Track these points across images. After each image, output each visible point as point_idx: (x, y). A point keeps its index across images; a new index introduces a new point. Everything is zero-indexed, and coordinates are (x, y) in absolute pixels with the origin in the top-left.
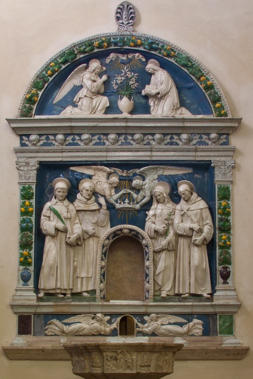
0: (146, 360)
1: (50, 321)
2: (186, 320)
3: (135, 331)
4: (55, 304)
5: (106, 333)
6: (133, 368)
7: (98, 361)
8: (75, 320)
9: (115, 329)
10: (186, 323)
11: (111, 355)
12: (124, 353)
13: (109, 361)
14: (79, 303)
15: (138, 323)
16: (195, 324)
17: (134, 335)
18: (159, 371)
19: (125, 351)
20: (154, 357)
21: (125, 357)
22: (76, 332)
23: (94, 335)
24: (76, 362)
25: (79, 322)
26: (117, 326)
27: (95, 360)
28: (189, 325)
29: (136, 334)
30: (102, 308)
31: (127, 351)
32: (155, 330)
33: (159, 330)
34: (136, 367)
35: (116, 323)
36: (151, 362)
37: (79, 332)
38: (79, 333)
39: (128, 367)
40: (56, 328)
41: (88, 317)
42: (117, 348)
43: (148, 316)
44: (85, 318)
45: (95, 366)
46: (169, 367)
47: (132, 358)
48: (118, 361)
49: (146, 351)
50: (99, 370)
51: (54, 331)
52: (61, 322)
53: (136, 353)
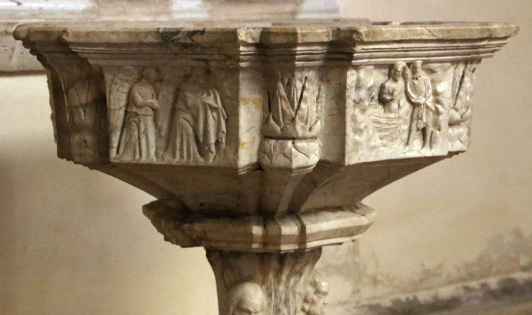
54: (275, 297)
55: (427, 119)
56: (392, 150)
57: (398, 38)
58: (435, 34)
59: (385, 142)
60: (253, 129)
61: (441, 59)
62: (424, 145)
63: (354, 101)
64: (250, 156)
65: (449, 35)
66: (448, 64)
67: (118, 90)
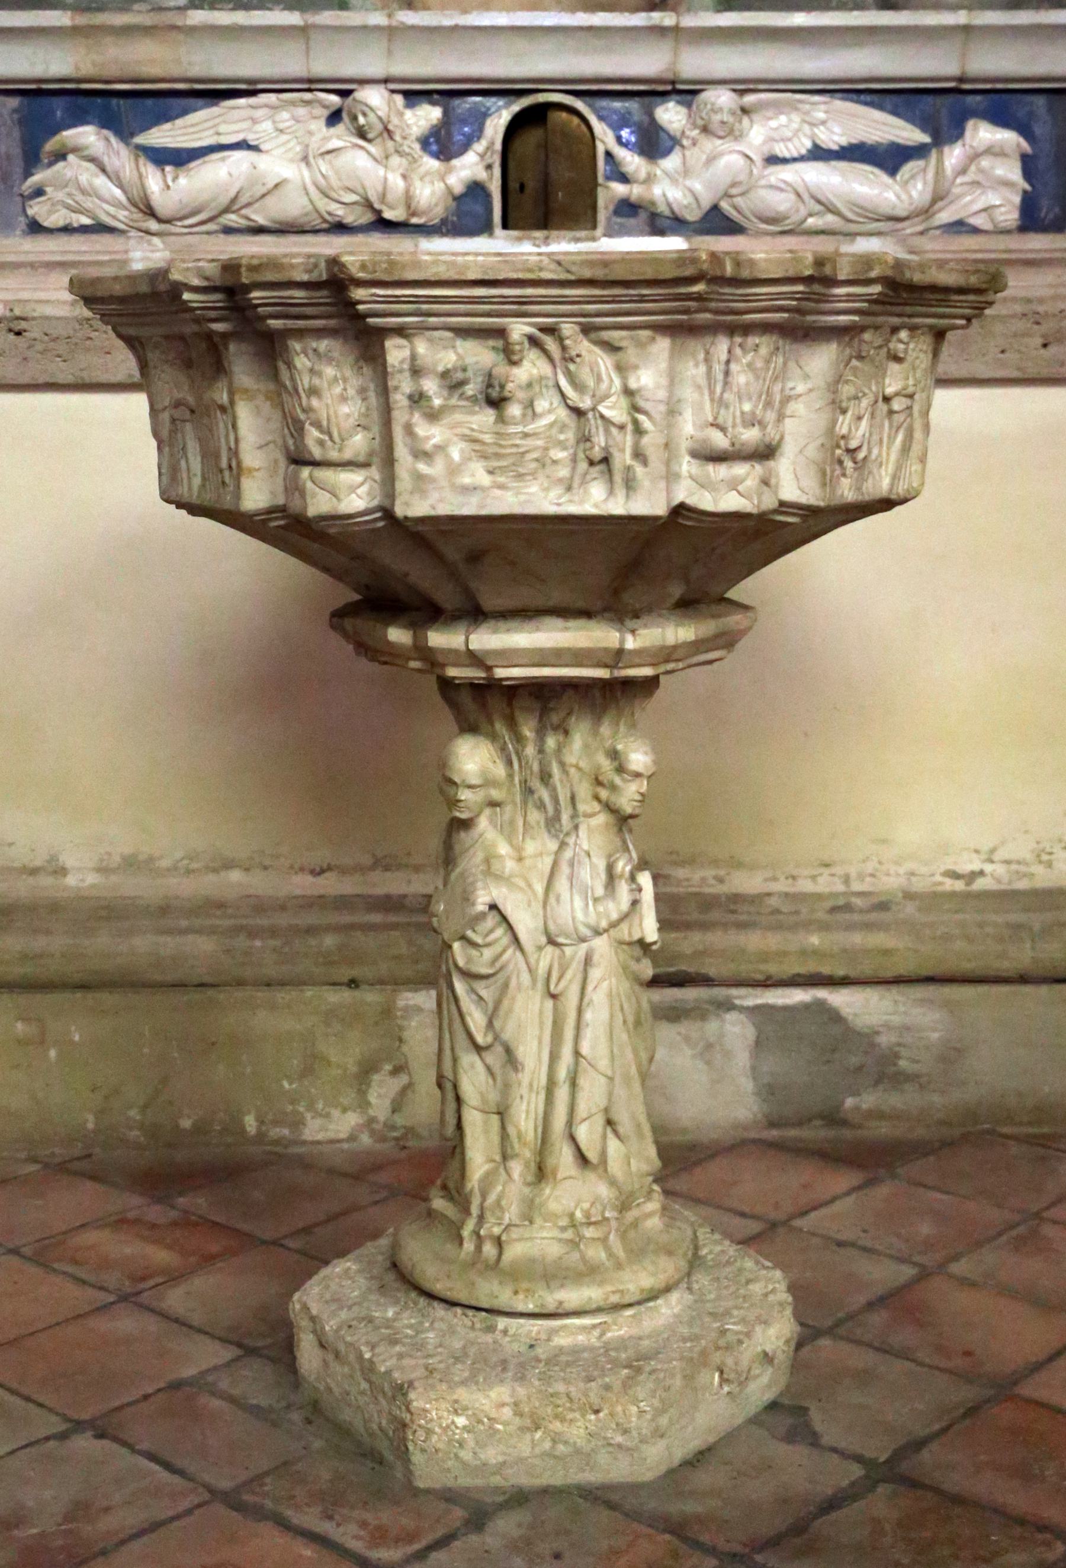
0: (747, 407)
1: (57, 138)
2: (924, 129)
3: (601, 202)
4: (82, 20)
5: (414, 214)
6: (639, 470)
7: (345, 409)
8: (222, 128)
9: (476, 190)
10: (918, 152)
11: (448, 359)
12: (561, 340)
13: (433, 416)
14: (240, 18)
15: (621, 153)
16: (975, 157)
17: (594, 227)
18: (847, 491)
19: (568, 328)
20: (806, 377)
21: (569, 375)
22: (227, 210)
23: (340, 228)
24: (173, 420)
25: (242, 145)
26: (489, 167)
27: (315, 402)
28: (940, 161)
29: (609, 220)
30: (390, 52)
31: (586, 330)
32: (727, 195)
33: (752, 195)
34: (668, 463)
35: (479, 147)
36: (781, 417)
37: (248, 205)
38: (244, 212)
39: (592, 463)
40: (101, 182)
41: (301, 111)
42: (505, 300)
43: (679, 102)
44: (285, 115)
45: (317, 453)
46: (906, 449)
47: (633, 384)
48: (514, 410)
49: (747, 329)
50: (353, 489)
51: (88, 203)
52: (127, 144)
53: (663, 344)
54: (520, 766)
55: (606, 442)
56: (522, 498)
57: (472, 276)
58: (574, 269)
59: (501, 479)
60: (272, 446)
61: (619, 323)
62: (611, 492)
63: (410, 397)
64: (272, 493)
65: (607, 271)
66: (645, 334)
67: (159, 379)
